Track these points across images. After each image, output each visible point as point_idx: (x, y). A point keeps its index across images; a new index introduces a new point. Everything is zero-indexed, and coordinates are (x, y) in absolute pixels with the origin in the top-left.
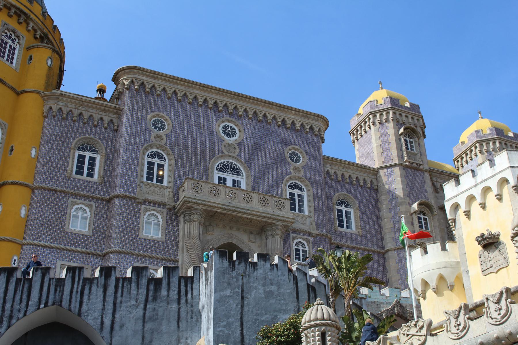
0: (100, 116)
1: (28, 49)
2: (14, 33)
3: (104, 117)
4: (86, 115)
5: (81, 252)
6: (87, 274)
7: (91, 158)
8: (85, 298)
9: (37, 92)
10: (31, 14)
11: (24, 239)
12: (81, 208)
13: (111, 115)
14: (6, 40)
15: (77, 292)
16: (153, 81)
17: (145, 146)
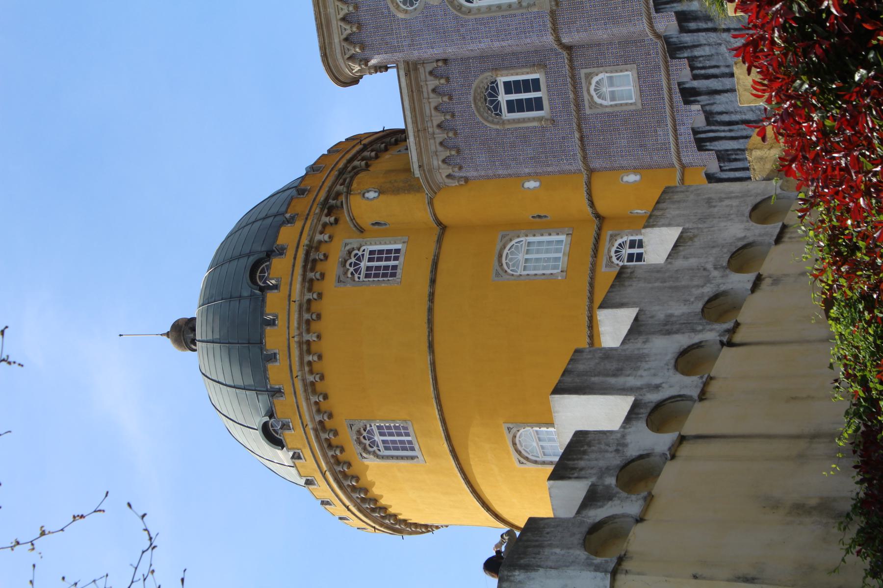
0: (432, 95)
1: (361, 230)
2: (346, 261)
3: (431, 87)
4: (438, 118)
5: (668, 75)
6: (700, 121)
7: (508, 91)
8: (734, 118)
9: (431, 203)
10: (302, 244)
11: (673, 166)
12: (595, 90)
13: (423, 77)
14: (363, 272)
15: (730, 131)
16: (335, 24)
17: (456, 12)
